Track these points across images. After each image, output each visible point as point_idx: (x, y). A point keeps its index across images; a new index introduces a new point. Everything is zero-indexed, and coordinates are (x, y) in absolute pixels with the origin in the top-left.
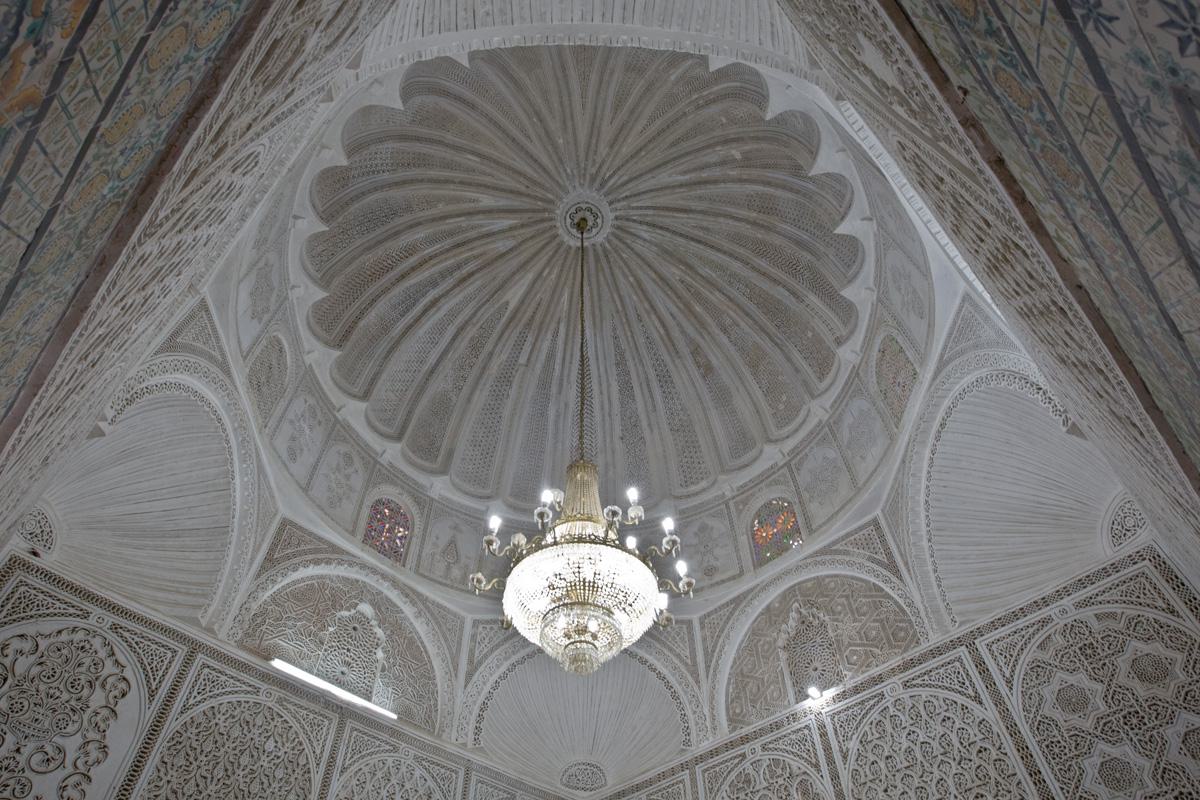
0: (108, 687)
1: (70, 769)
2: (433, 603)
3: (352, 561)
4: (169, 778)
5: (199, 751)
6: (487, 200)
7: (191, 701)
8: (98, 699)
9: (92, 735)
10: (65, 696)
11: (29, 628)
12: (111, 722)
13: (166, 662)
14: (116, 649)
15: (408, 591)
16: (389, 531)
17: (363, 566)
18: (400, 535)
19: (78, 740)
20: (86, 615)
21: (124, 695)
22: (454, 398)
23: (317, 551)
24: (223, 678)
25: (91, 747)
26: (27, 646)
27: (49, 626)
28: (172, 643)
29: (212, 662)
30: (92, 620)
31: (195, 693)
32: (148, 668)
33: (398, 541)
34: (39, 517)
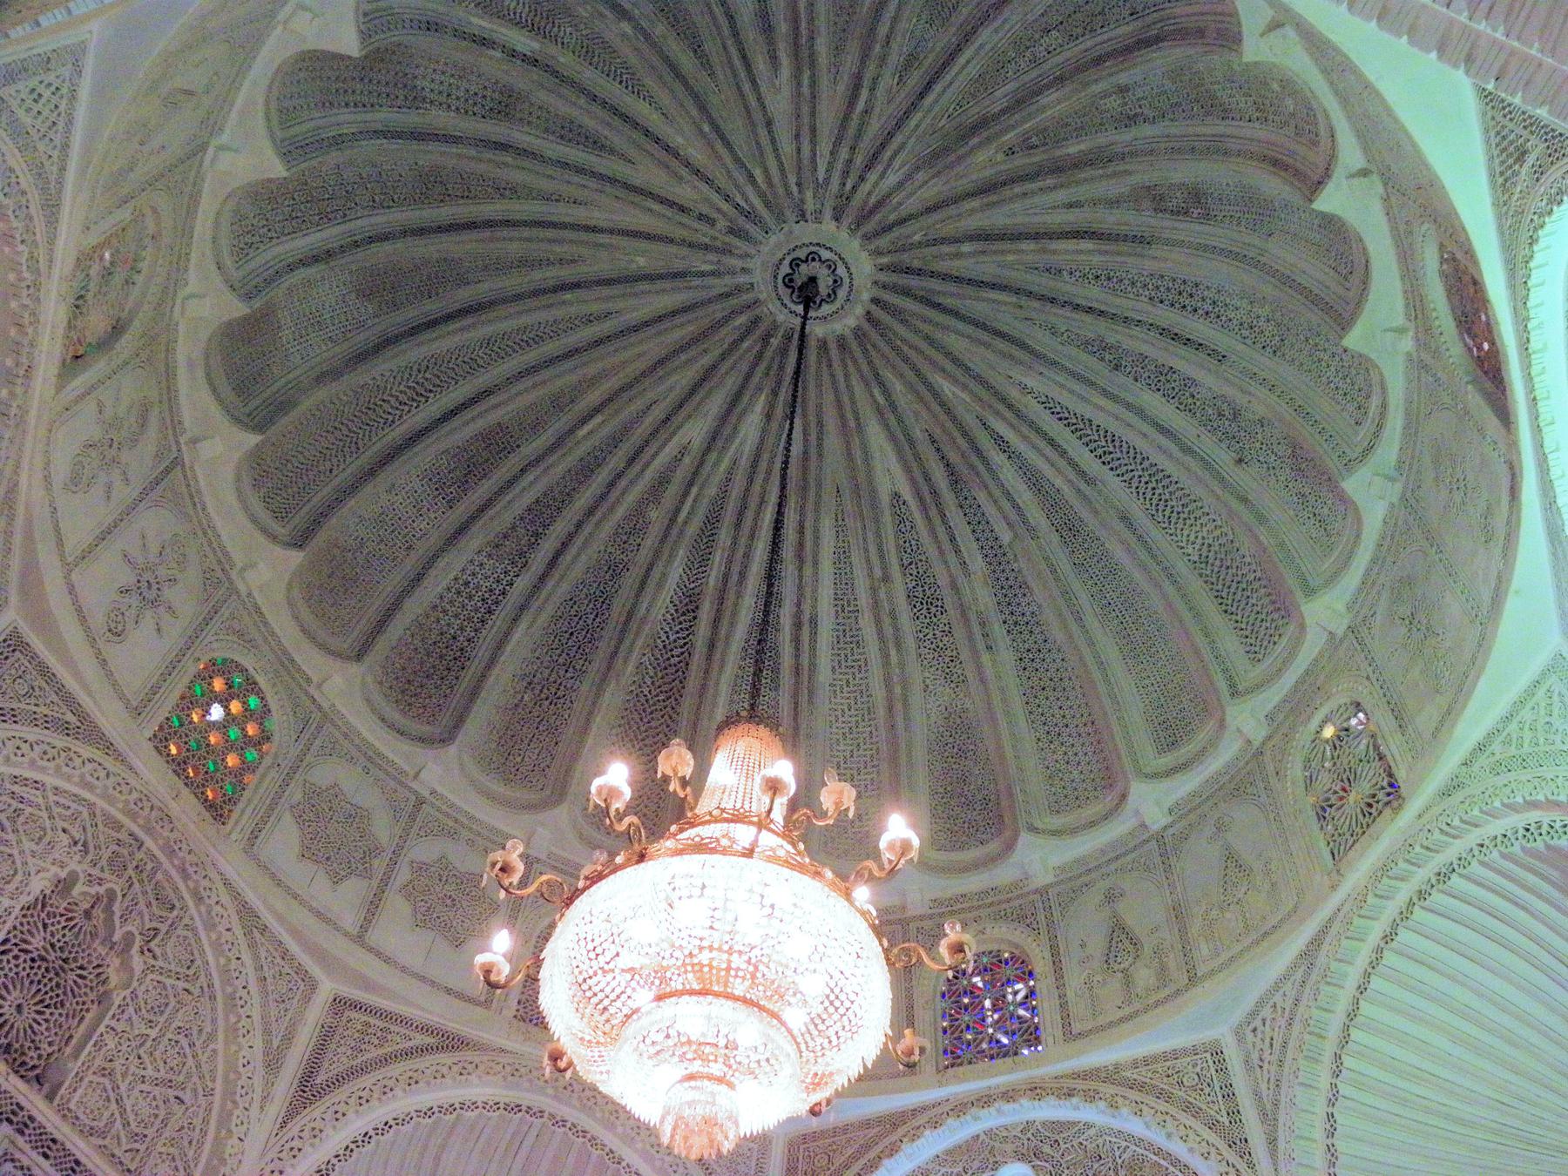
2: (1135, 1064)
3: (933, 1116)
6: (694, 432)
15: (1071, 1083)
16: (995, 1009)
17: (960, 1108)
18: (1020, 997)
22: (968, 705)
23: (867, 1147)
33: (1021, 1012)
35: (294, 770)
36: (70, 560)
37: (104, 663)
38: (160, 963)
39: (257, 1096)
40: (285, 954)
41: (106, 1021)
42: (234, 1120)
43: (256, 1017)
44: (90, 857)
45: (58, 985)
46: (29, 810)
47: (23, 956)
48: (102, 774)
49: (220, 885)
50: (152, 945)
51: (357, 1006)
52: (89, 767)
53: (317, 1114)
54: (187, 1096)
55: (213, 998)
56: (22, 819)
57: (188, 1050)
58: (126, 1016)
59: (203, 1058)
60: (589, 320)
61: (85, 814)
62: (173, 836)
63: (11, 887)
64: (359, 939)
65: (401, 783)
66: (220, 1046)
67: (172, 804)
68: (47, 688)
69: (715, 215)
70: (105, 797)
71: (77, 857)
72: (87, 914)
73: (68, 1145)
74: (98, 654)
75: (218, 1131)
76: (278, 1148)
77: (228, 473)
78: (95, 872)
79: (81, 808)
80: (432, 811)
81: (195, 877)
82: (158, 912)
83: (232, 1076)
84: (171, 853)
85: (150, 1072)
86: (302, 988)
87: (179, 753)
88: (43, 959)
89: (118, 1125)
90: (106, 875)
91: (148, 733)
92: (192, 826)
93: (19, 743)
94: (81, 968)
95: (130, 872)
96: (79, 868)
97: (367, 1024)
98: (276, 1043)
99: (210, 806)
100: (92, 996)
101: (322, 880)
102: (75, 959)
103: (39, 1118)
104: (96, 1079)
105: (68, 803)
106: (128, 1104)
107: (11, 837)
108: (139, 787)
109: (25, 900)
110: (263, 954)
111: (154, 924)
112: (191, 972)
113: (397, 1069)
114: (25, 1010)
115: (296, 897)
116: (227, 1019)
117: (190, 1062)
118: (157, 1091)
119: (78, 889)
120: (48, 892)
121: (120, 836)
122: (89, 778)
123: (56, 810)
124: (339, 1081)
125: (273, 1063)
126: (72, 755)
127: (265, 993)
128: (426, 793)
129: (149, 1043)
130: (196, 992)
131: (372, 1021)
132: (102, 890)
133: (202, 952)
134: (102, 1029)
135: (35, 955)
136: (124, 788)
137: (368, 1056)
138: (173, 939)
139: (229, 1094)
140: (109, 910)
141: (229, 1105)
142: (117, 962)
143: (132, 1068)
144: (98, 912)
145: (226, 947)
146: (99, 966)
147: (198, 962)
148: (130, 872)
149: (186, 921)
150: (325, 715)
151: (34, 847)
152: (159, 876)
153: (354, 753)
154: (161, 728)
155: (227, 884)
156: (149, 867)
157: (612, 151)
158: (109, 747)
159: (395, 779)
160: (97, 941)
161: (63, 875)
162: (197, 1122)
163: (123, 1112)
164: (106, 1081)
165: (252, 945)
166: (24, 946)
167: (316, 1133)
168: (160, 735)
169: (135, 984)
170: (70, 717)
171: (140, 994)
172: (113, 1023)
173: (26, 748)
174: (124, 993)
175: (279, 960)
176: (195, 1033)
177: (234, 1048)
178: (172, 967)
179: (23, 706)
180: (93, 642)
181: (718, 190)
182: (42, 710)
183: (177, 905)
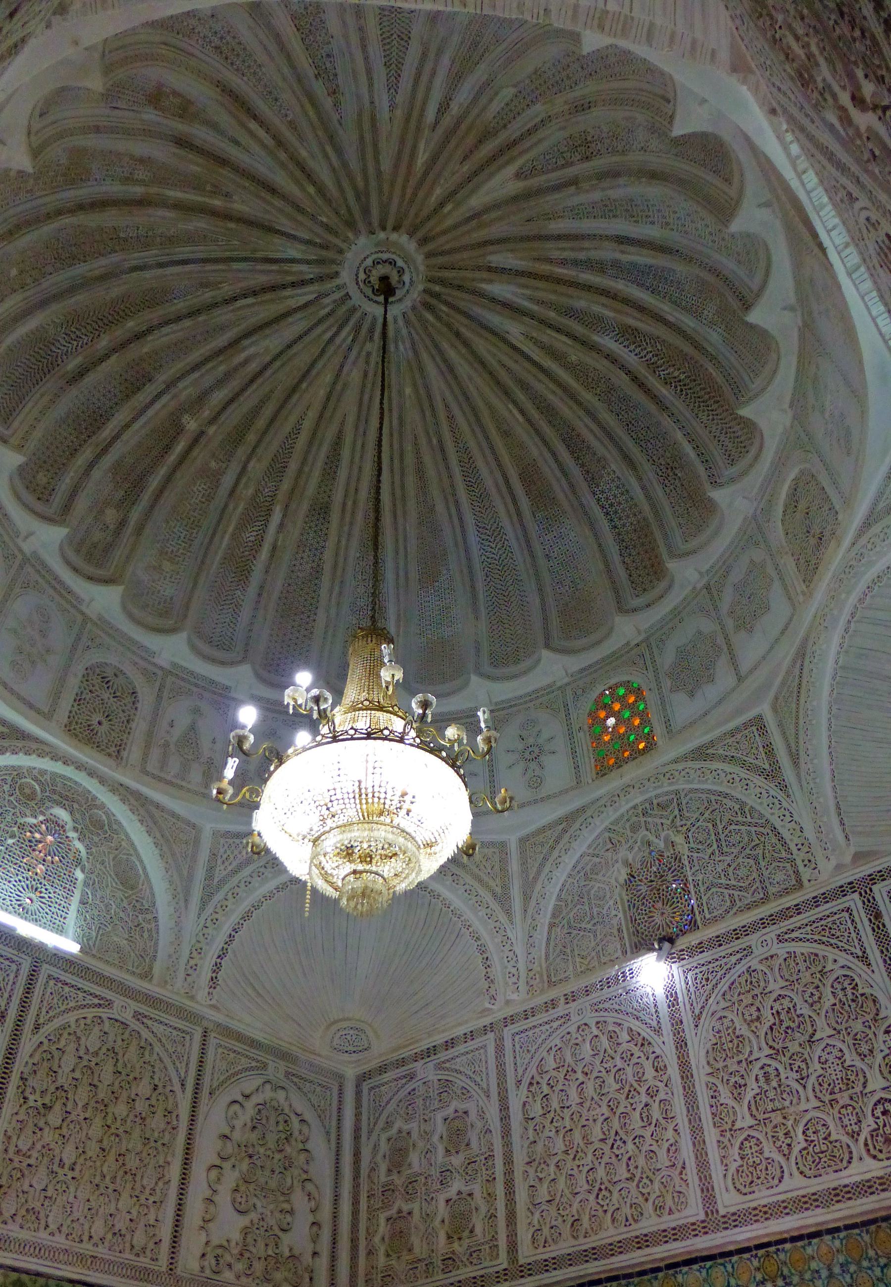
6: (514, 330)
40: (732, 734)
57: (737, 827)
60: (451, 418)
64: (740, 679)
69: (364, 353)
77: (497, 686)
123: (596, 852)
133: (703, 791)
155: (676, 761)
157: (340, 432)
163: (734, 887)
181: (345, 358)
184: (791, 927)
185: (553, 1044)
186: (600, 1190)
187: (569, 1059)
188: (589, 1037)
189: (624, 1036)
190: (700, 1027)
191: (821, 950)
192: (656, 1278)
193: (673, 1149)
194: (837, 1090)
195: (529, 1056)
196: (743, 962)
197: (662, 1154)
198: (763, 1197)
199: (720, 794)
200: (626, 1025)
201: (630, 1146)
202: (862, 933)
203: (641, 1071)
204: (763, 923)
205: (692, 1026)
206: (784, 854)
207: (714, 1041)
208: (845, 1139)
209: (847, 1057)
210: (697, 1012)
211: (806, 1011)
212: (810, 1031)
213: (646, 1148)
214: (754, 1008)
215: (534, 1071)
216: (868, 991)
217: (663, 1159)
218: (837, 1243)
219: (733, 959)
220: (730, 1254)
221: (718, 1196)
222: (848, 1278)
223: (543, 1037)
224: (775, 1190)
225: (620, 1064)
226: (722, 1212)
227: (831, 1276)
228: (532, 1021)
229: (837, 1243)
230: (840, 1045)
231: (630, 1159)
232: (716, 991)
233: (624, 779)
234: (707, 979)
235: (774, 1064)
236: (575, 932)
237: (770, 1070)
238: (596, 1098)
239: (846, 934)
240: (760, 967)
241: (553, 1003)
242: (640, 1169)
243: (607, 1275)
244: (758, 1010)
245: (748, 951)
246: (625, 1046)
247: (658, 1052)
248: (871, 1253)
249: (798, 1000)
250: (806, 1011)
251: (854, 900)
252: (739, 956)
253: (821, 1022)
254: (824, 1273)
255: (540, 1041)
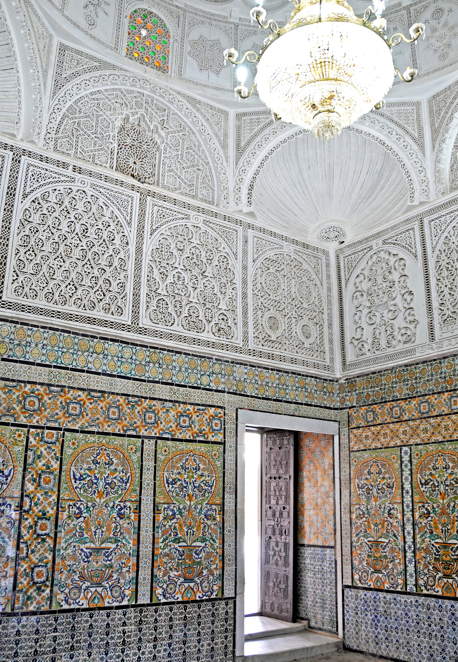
0: (397, 268)
1: (404, 310)
4: (445, 284)
5: (452, 262)
7: (434, 243)
8: (395, 276)
9: (403, 292)
10: (385, 285)
11: (358, 271)
12: (407, 280)
13: (412, 237)
14: (390, 251)
19: (399, 297)
20: (371, 248)
21: (405, 265)
24: (443, 219)
25: (406, 296)
26: (362, 277)
27: (363, 264)
28: (409, 226)
29: (433, 217)
30: (375, 247)
31: (434, 238)
32: (407, 246)
34: (332, 229)
35: (183, 39)
36: (60, 8)
37: (95, 38)
38: (170, 130)
39: (224, 158)
40: (212, 108)
41: (163, 156)
42: (219, 169)
43: (210, 132)
44: (129, 107)
45: (142, 151)
46: (101, 101)
47: (127, 147)
48: (117, 77)
49: (176, 95)
50: (164, 125)
51: (245, 114)
52: (111, 77)
53: (246, 156)
54: (201, 167)
55: (194, 133)
56: (101, 106)
57: (193, 153)
58: (168, 151)
59: (200, 154)
61: (120, 93)
62: (151, 86)
63: (110, 129)
65: (226, 22)
66: (204, 147)
67: (145, 75)
68: (82, 58)
70: (122, 84)
71: (125, 109)
72: (139, 125)
73: (170, 196)
74: (91, 36)
75: (216, 174)
76: (238, 172)
78: (133, 111)
79: (117, 92)
80: (243, 27)
81: (166, 96)
82: (161, 114)
83: (212, 155)
84: (155, 93)
85: (185, 165)
86: (223, 116)
87: (139, 56)
88: (133, 145)
89: (183, 184)
90: (137, 110)
91: (124, 54)
92: (156, 79)
93: (85, 82)
94: (146, 142)
95: (144, 105)
96: (127, 112)
97: (251, 119)
98: (222, 139)
99: (159, 68)
100: (155, 150)
101: (213, 77)
102: (143, 141)
103: (157, 192)
104: (168, 174)
105: (112, 93)
106: (183, 177)
107: (101, 113)
108: (131, 75)
109: (117, 131)
110: (203, 111)
111: (162, 118)
112: (182, 128)
113: (267, 131)
114: (137, 162)
115: (205, 86)
116: (201, 138)
117: (196, 156)
118: (190, 170)
119: (131, 119)
120: (123, 124)
121: (134, 95)
122: (113, 81)
123: (109, 97)
124: (249, 143)
125: (225, 146)
126: (103, 76)
127: (210, 124)
128: (237, 21)
129: (180, 156)
130: (187, 134)
131: (253, 117)
132: (138, 116)
133: (183, 120)
134: (162, 159)
135: (130, 145)
136: (127, 78)
137: (256, 130)
138: (171, 120)
139: (214, 161)
140: (144, 120)
141: (216, 165)
142: (157, 136)
143: (179, 166)
144: (142, 123)
145: (189, 115)
146: (152, 140)
147: (183, 124)
148: (144, 105)
149: (172, 112)
150: (184, 10)
151: (110, 113)
152: (155, 102)
153: (202, 19)
154: (128, 50)
155: (179, 93)
156: (150, 100)
158: (114, 67)
159: (223, 22)
160: (147, 132)
161: (124, 117)
162: (208, 174)
163: (182, 180)
164: (172, 173)
165: (198, 110)
166: (125, 144)
167: (249, 163)
168: (129, 53)
169: (165, 140)
170: (95, 64)
171: (169, 142)
172: (165, 155)
173: (88, 82)
174: (163, 145)
175: (210, 110)
176: (193, 146)
177: (208, 146)
178: (175, 129)
179: (79, 69)
180: (86, 33)
182: (85, 66)
183: (166, 109)
184: (211, 221)
185: (58, 188)
186: (69, 284)
187: (66, 203)
188: (84, 200)
189: (108, 214)
190: (153, 236)
191: (220, 240)
192: (93, 341)
193: (122, 286)
194: (207, 300)
195: (39, 185)
196: (184, 220)
197: (114, 284)
198: (161, 327)
199: (191, 129)
200: (111, 208)
201: (95, 271)
202: (238, 244)
203: (113, 237)
204: (198, 209)
205: (149, 234)
206: (211, 184)
207: (158, 247)
208: (204, 321)
209: (215, 289)
210: (154, 228)
211: (205, 260)
212: (204, 270)
213: (105, 276)
214: (182, 245)
215: (39, 195)
216: (232, 269)
217: (114, 287)
218: (187, 359)
219: (180, 216)
220: (137, 345)
221: (140, 318)
222: (187, 374)
223: (51, 180)
224: (168, 328)
225: (101, 226)
226: (140, 325)
227: (180, 371)
228: (44, 165)
229: (187, 359)
230: (214, 283)
231: (92, 277)
232: (167, 225)
233: (145, 75)
234: (164, 216)
235: (184, 275)
236: (81, 132)
237: (181, 276)
238: (79, 234)
239: (232, 240)
240: (191, 228)
241: (65, 165)
242: (98, 286)
243: (62, 328)
244: (184, 246)
245: (187, 217)
246: (106, 219)
247: (126, 234)
248: (199, 368)
249: (203, 253)
250: (205, 260)
251: (240, 229)
252: (183, 216)
253: (209, 269)
254: (178, 369)
255: (49, 181)
